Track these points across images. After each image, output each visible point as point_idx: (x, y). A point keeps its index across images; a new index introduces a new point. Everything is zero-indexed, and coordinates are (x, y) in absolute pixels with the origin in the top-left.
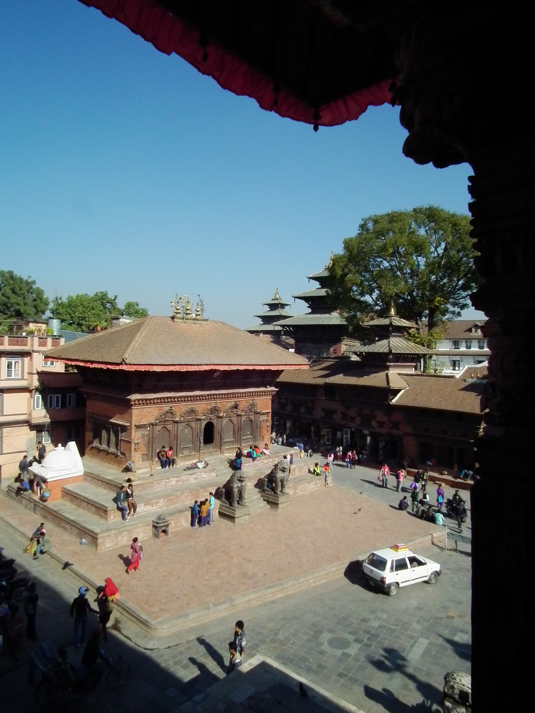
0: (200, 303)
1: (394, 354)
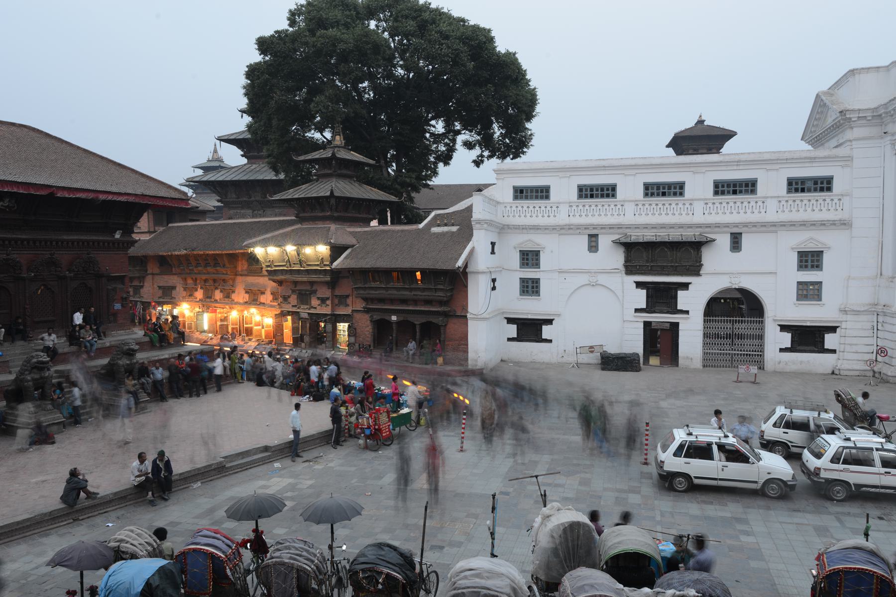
1: (339, 198)
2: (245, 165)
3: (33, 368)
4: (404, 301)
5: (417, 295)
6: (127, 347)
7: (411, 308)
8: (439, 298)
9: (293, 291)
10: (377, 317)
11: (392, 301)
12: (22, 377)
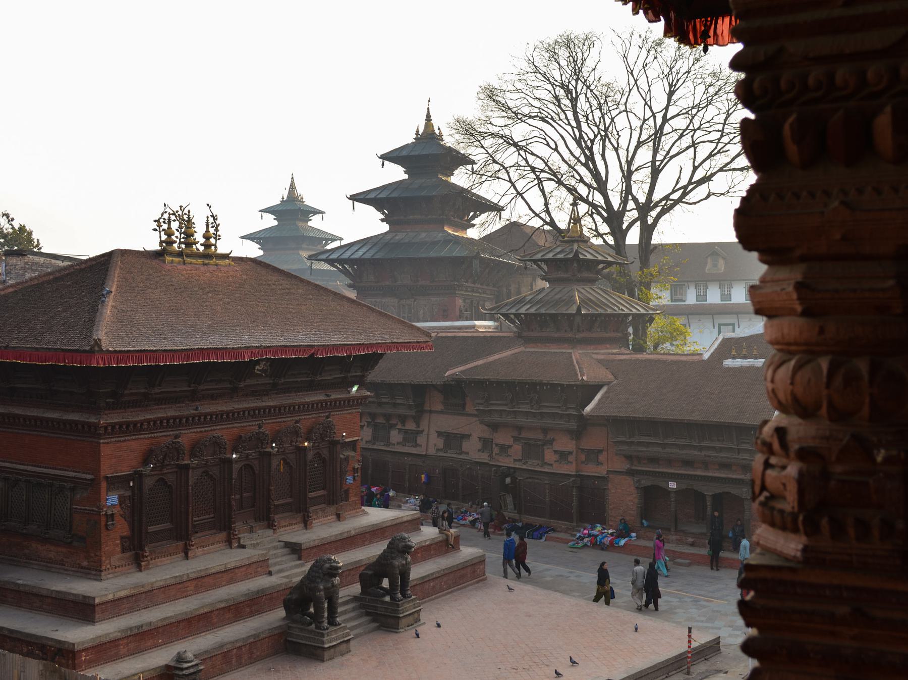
0: (211, 220)
2: (386, 233)
3: (324, 575)
4: (688, 463)
5: (709, 456)
6: (404, 544)
7: (699, 473)
8: (744, 462)
9: (516, 439)
10: (646, 482)
11: (670, 462)
12: (313, 585)
